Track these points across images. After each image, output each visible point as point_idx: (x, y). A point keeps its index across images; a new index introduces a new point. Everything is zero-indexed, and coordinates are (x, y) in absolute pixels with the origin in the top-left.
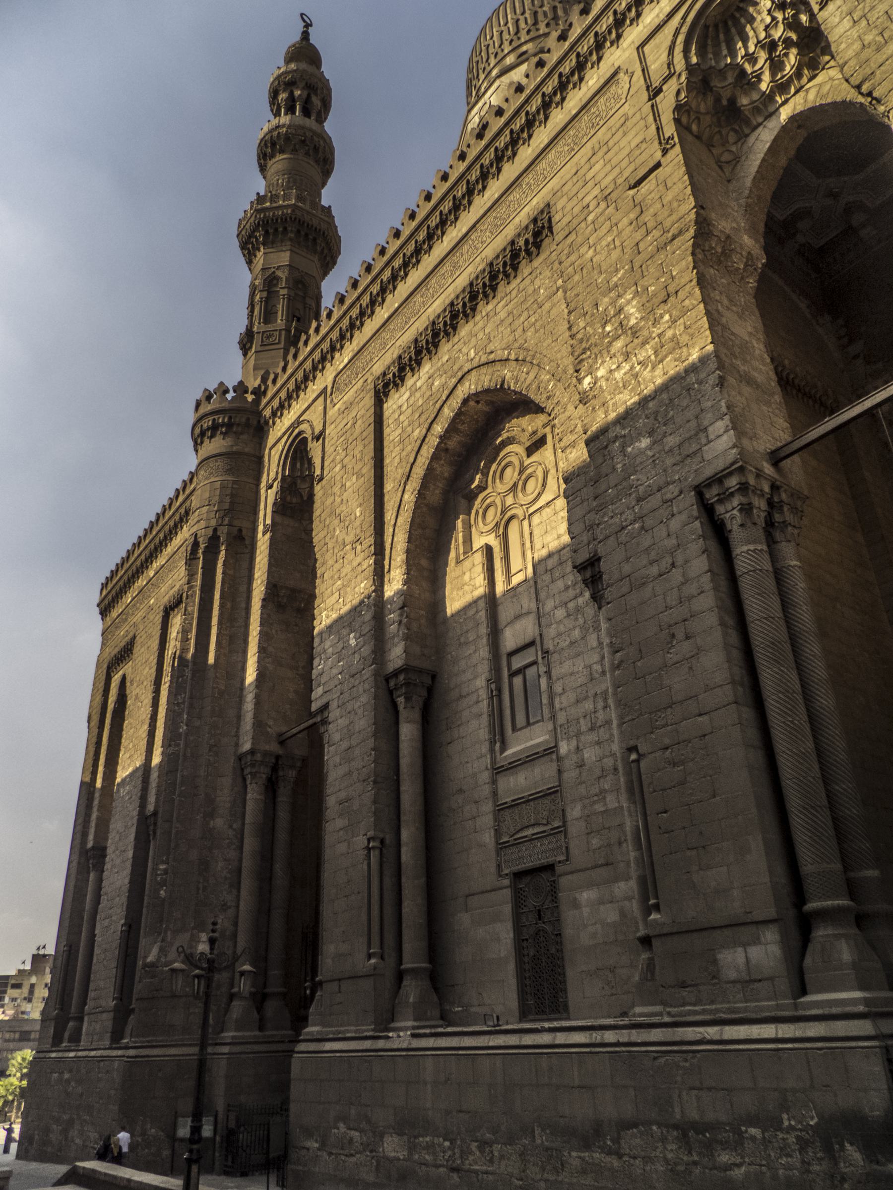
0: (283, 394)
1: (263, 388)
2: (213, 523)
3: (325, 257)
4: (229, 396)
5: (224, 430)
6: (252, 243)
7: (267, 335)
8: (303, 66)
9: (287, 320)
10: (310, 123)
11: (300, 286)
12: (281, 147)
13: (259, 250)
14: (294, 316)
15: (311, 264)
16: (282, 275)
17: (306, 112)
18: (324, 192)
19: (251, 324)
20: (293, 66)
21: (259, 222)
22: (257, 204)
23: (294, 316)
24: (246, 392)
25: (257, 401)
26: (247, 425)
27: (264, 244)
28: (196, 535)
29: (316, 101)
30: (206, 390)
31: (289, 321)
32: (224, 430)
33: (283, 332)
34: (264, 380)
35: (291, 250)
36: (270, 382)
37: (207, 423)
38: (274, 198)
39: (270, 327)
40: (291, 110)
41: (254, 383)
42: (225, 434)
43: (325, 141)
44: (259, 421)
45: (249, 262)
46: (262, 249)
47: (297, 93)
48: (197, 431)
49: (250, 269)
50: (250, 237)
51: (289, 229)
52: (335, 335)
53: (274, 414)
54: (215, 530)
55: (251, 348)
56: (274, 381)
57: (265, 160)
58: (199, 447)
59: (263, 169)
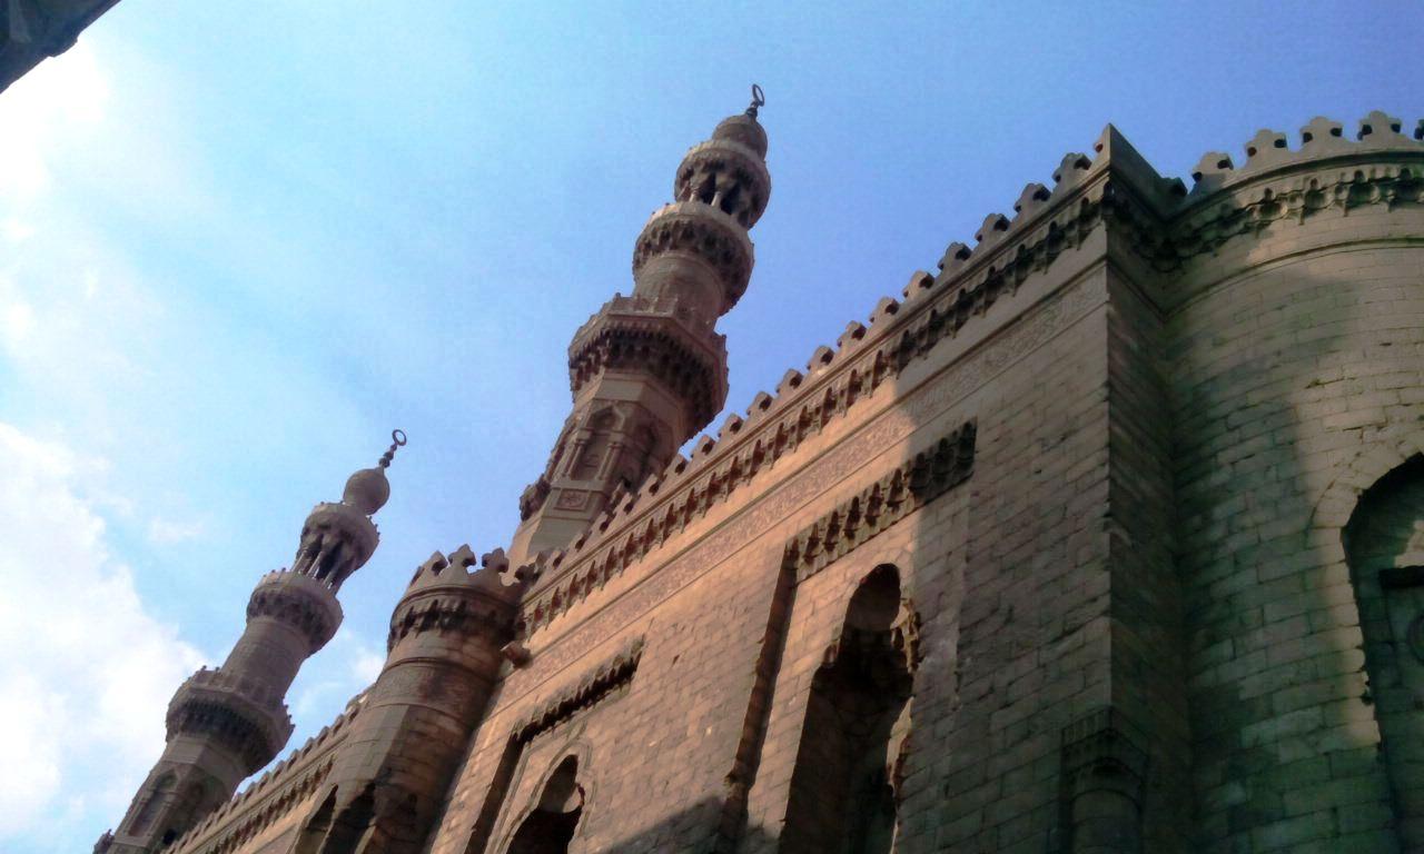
0: (565, 584)
1: (536, 571)
2: (371, 774)
3: (697, 406)
4: (471, 569)
5: (446, 620)
6: (590, 360)
8: (741, 148)
10: (730, 221)
11: (645, 437)
13: (597, 373)
14: (622, 477)
15: (670, 409)
17: (726, 206)
18: (720, 319)
20: (725, 143)
21: (608, 333)
22: (613, 308)
23: (622, 477)
24: (503, 568)
25: (518, 590)
26: (489, 622)
27: (608, 365)
28: (336, 788)
29: (745, 197)
30: (438, 553)
31: (611, 481)
32: (446, 620)
33: (597, 498)
34: (541, 559)
35: (646, 382)
36: (549, 562)
37: (423, 605)
38: (640, 302)
39: (577, 485)
40: (706, 196)
41: (520, 559)
42: (446, 629)
43: (743, 252)
44: (512, 621)
45: (576, 388)
46: (602, 370)
47: (721, 179)
48: (403, 615)
49: (574, 401)
50: (589, 350)
51: (653, 350)
52: (681, 500)
53: (538, 614)
54: (371, 786)
55: (538, 509)
56: (557, 562)
57: (646, 253)
58: (396, 641)
59: (638, 264)
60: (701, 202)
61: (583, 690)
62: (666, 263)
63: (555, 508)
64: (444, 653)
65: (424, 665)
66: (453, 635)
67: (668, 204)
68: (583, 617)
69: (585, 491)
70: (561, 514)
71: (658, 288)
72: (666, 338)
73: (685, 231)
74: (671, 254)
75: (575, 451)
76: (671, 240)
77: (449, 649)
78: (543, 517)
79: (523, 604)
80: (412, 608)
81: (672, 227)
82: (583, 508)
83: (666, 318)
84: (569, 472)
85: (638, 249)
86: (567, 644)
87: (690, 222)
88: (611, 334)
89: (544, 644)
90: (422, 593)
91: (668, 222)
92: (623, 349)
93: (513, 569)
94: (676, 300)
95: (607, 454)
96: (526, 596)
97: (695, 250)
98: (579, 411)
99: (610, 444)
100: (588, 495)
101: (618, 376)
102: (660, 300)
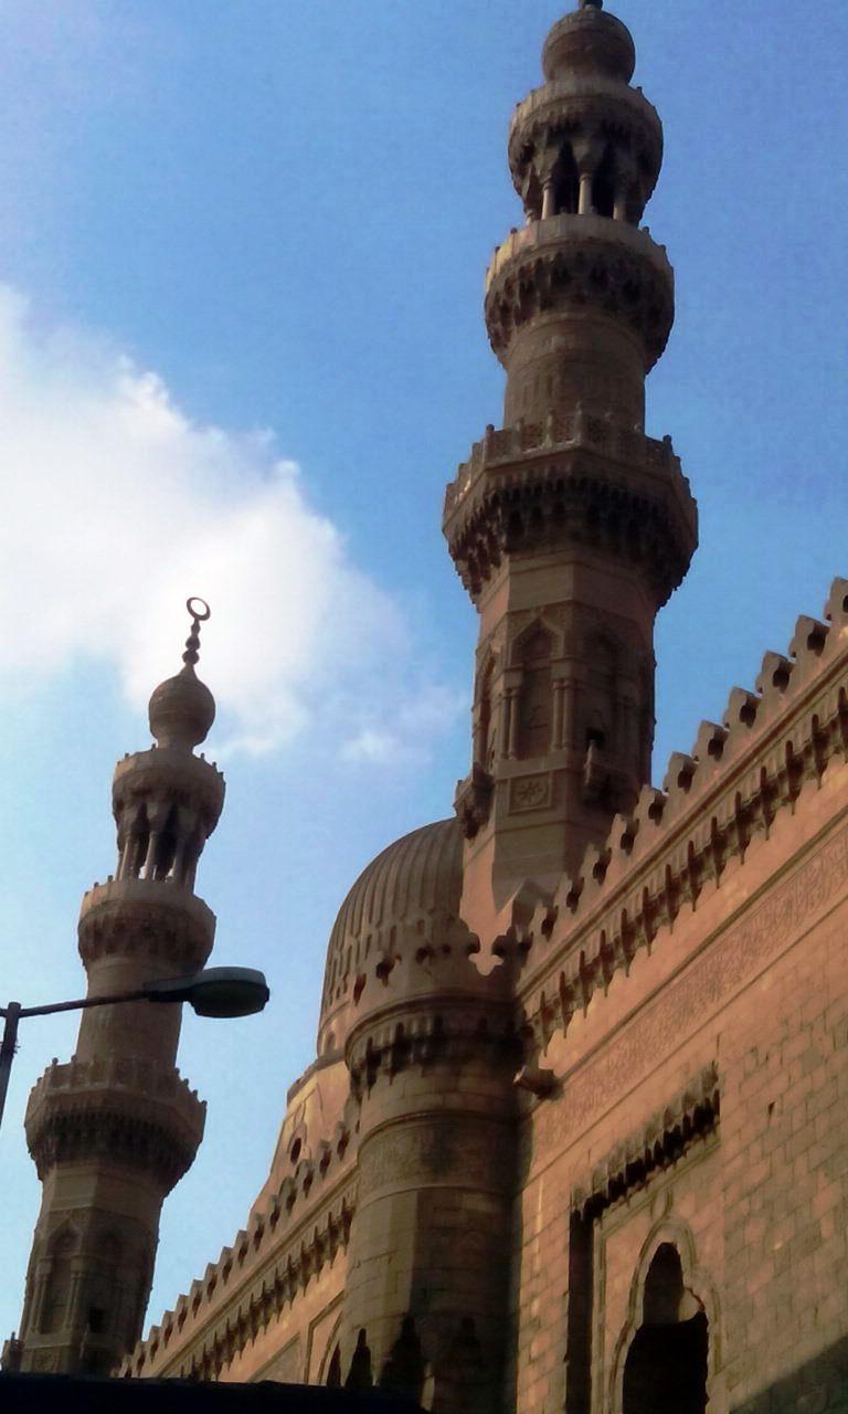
1: (519, 939)
6: (480, 545)
7: (522, 788)
9: (574, 747)
16: (559, 630)
19: (483, 754)
25: (505, 976)
31: (577, 748)
34: (521, 914)
36: (536, 925)
42: (427, 1063)
51: (569, 507)
55: (486, 818)
56: (548, 926)
57: (506, 323)
59: (499, 341)
61: (652, 1147)
62: (540, 338)
63: (510, 815)
64: (435, 1100)
65: (416, 1124)
66: (440, 1070)
67: (514, 231)
68: (613, 1022)
70: (521, 822)
71: (543, 386)
73: (555, 273)
74: (545, 320)
75: (509, 708)
76: (538, 294)
77: (440, 1092)
78: (498, 833)
79: (519, 998)
81: (534, 271)
82: (549, 805)
83: (576, 450)
84: (511, 749)
85: (490, 320)
86: (604, 1062)
87: (559, 255)
88: (501, 497)
89: (567, 1064)
90: (377, 1017)
91: (525, 264)
92: (526, 517)
93: (487, 943)
94: (580, 413)
96: (520, 986)
97: (580, 300)
98: (492, 636)
99: (555, 685)
100: (550, 781)
101: (533, 563)
102: (556, 421)
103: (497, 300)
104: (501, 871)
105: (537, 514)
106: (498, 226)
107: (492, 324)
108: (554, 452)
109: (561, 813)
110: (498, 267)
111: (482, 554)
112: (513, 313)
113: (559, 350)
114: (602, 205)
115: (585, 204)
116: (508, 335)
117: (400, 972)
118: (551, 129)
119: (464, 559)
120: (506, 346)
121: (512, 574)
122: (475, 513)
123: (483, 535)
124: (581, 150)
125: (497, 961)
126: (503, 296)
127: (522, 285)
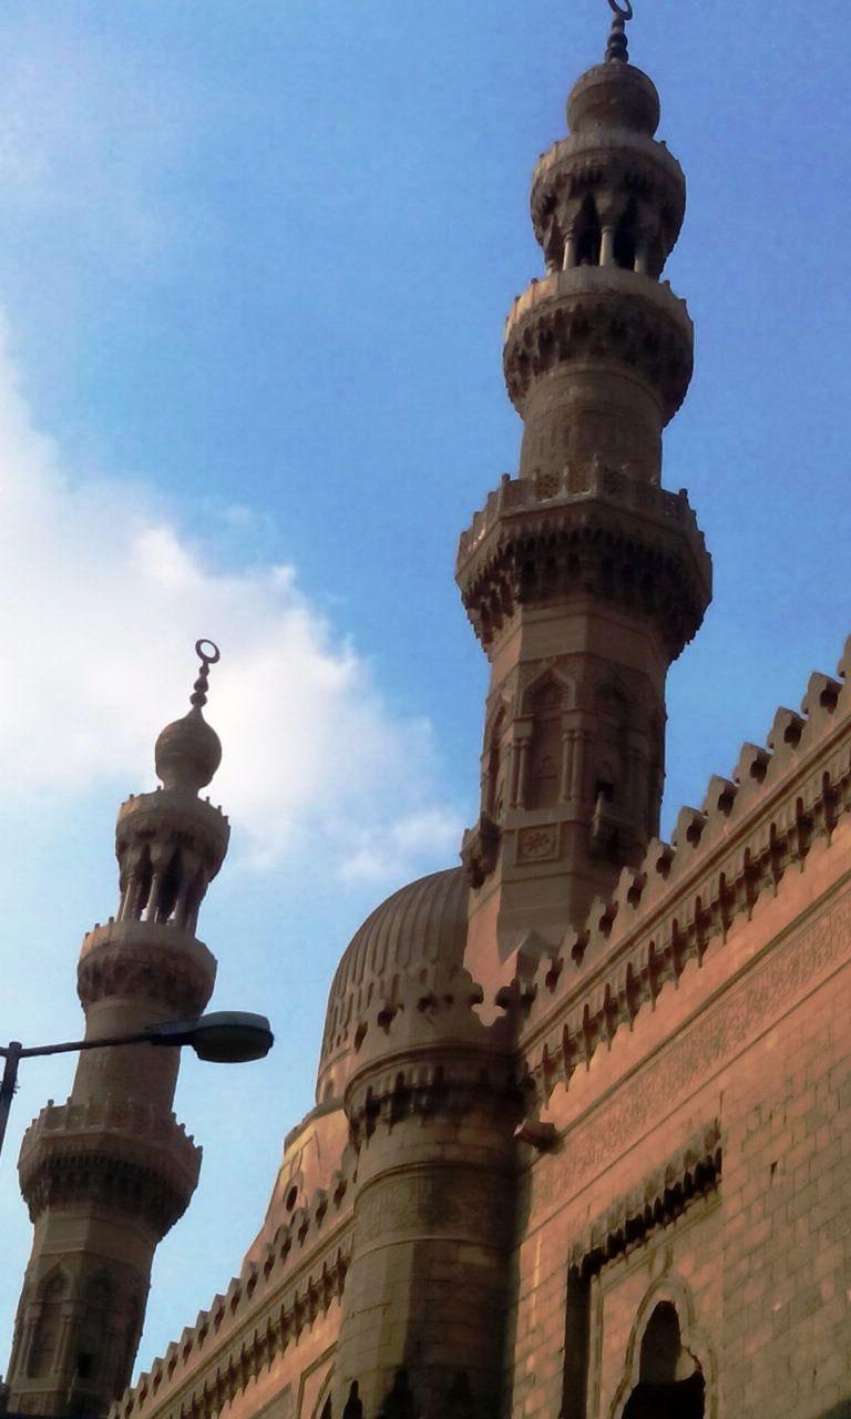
1: (523, 990)
7: (529, 839)
9: (582, 799)
12: (562, 343)
16: (570, 680)
19: (491, 804)
25: (508, 1027)
31: (586, 801)
34: (526, 965)
36: (540, 978)
42: (427, 1113)
56: (552, 978)
57: (524, 373)
59: (516, 391)
60: (584, 267)
61: (652, 1203)
62: (558, 387)
63: (519, 865)
64: (433, 1151)
65: (414, 1175)
66: (440, 1120)
67: (535, 281)
68: (616, 1076)
69: (554, 825)
71: (560, 436)
72: (599, 532)
73: (575, 324)
74: (563, 370)
75: (518, 757)
76: (557, 345)
78: (505, 883)
79: (521, 1050)
80: (370, 1090)
81: (553, 323)
82: (557, 854)
83: (590, 501)
86: (606, 1117)
87: (579, 307)
88: (515, 549)
90: (377, 1067)
91: (544, 314)
92: (540, 568)
93: (490, 995)
94: (596, 464)
95: (565, 754)
96: (522, 1038)
97: (598, 352)
98: (503, 685)
99: (565, 736)
101: (547, 613)
102: (571, 472)
103: (516, 349)
104: (506, 923)
105: (551, 563)
106: (520, 277)
107: (510, 374)
108: (569, 502)
109: (568, 865)
110: (518, 317)
111: (495, 603)
112: (531, 363)
113: (576, 401)
114: (623, 257)
115: (606, 255)
116: (526, 383)
117: (401, 1022)
118: (574, 180)
119: (476, 608)
120: (523, 395)
121: (525, 624)
122: (490, 563)
123: (497, 584)
124: (603, 202)
125: (500, 1012)
126: (522, 346)
127: (541, 335)
